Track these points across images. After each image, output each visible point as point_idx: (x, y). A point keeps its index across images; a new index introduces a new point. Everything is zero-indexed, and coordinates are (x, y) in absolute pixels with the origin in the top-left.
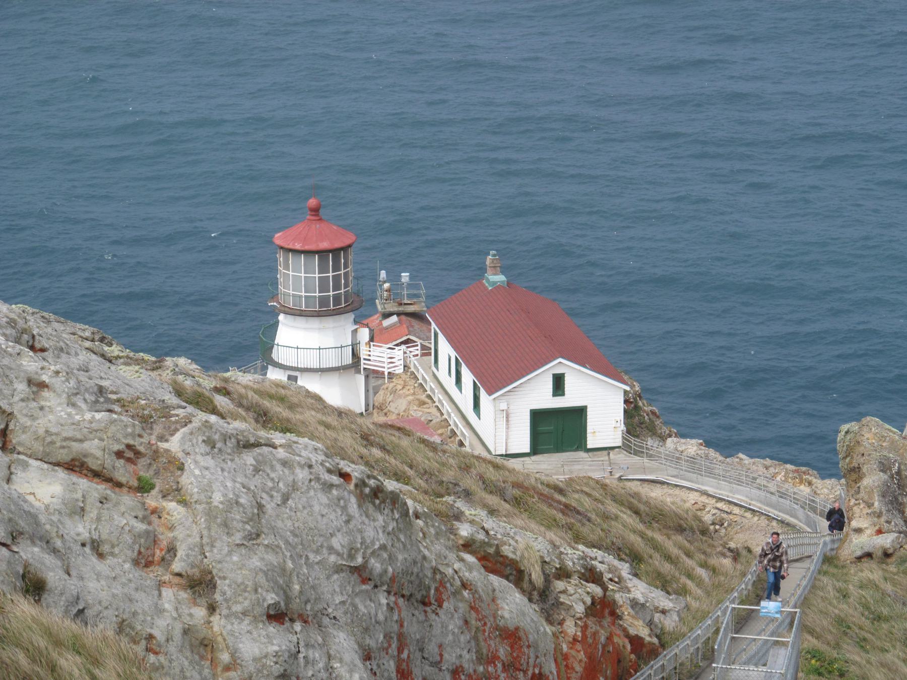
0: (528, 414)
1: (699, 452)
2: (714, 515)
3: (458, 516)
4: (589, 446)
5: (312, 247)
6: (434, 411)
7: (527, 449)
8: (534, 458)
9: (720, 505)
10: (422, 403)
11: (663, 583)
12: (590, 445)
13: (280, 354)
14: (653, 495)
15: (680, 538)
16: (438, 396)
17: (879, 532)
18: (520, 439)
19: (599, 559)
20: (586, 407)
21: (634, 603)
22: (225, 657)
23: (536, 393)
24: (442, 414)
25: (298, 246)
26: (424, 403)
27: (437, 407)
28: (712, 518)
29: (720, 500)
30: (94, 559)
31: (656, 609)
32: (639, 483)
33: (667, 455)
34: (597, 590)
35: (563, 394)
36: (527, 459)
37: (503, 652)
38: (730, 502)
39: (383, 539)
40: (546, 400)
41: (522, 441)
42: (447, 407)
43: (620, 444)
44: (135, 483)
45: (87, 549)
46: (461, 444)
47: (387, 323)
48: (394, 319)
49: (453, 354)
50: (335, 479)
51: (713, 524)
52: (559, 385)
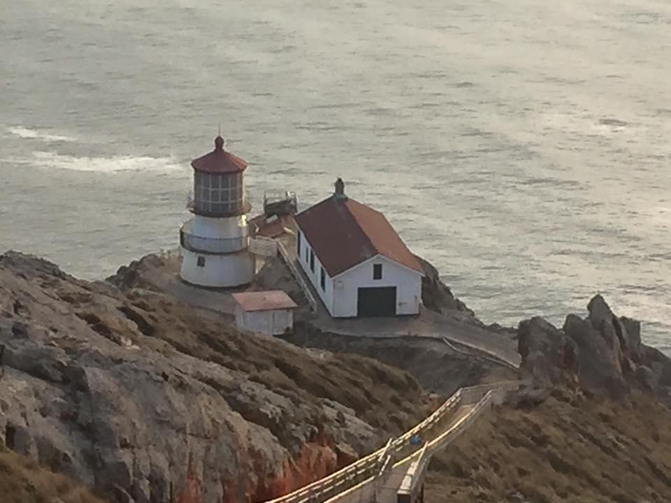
0: (356, 292)
3: (238, 389)
4: (397, 313)
10: (288, 280)
11: (374, 423)
14: (435, 349)
15: (393, 392)
16: (298, 275)
17: (536, 388)
18: (349, 307)
19: (336, 407)
20: (395, 288)
21: (348, 434)
22: (100, 465)
23: (361, 276)
24: (300, 287)
25: (207, 169)
27: (297, 283)
30: (40, 416)
31: (363, 438)
34: (316, 429)
35: (380, 278)
37: (250, 462)
39: (183, 407)
40: (369, 282)
42: (303, 283)
43: (417, 312)
44: (60, 379)
45: (38, 412)
47: (269, 220)
48: (275, 217)
49: (310, 248)
50: (160, 378)
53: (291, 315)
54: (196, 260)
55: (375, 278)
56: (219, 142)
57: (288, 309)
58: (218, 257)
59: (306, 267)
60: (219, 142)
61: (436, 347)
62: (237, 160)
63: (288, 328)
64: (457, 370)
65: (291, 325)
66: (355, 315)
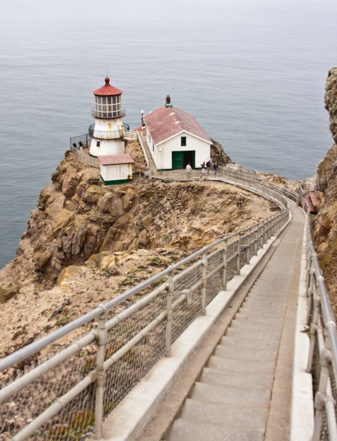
5: (105, 94)
6: (141, 153)
7: (171, 168)
8: (174, 171)
9: (244, 192)
13: (95, 134)
25: (100, 94)
26: (138, 150)
29: (243, 189)
36: (170, 171)
38: (248, 191)
41: (168, 164)
46: (146, 165)
53: (131, 168)
54: (96, 144)
56: (107, 81)
57: (129, 164)
58: (106, 142)
59: (148, 141)
60: (107, 81)
62: (117, 90)
63: (129, 176)
64: (230, 200)
65: (131, 174)
66: (171, 168)
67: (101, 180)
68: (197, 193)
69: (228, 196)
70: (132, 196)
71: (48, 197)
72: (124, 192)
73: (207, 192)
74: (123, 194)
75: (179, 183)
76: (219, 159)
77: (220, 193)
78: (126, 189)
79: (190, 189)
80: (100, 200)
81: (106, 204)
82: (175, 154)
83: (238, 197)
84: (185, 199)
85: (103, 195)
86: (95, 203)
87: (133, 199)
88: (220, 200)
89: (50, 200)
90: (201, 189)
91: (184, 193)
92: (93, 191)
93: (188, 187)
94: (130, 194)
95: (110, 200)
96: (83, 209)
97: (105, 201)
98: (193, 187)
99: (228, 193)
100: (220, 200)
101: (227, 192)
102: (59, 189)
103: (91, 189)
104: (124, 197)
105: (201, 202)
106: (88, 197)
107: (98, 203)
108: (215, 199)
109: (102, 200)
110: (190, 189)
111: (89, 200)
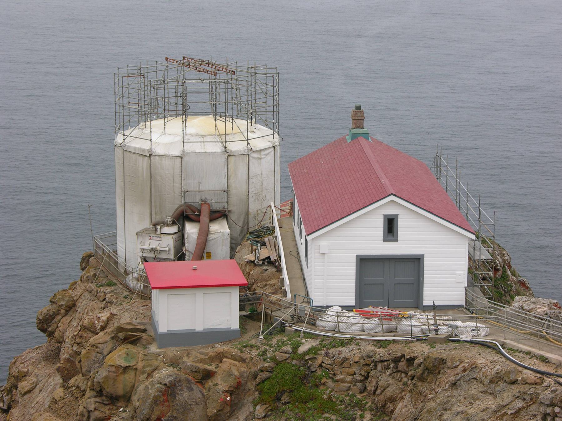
0: (354, 260)
1: (548, 312)
2: (554, 391)
7: (353, 303)
12: (427, 301)
20: (423, 256)
23: (362, 234)
28: (550, 396)
32: (468, 345)
33: (512, 315)
43: (461, 300)
51: (552, 405)
52: (391, 227)
55: (384, 240)
61: (483, 358)
64: (520, 404)
66: (353, 303)
67: (151, 332)
68: (422, 379)
69: (515, 389)
70: (232, 382)
71: (23, 376)
72: (212, 368)
73: (449, 376)
74: (208, 375)
75: (371, 348)
76: (493, 280)
77: (491, 381)
78: (219, 358)
79: (402, 365)
80: (141, 388)
81: (156, 401)
82: (364, 263)
83: (546, 396)
84: (388, 393)
85: (150, 375)
86: (127, 398)
87: (237, 390)
88: (491, 403)
89: (24, 385)
90: (434, 368)
91: (385, 378)
92: (124, 364)
93: (397, 360)
94: (230, 374)
95: (170, 390)
96: (89, 412)
97: (153, 391)
98: (411, 361)
99: (514, 382)
100: (491, 403)
101: (512, 377)
102: (52, 356)
103: (119, 357)
104: (210, 383)
105: (432, 404)
106: (106, 377)
107: (135, 398)
108: (474, 398)
109: (147, 389)
110: (401, 363)
111: (109, 389)
